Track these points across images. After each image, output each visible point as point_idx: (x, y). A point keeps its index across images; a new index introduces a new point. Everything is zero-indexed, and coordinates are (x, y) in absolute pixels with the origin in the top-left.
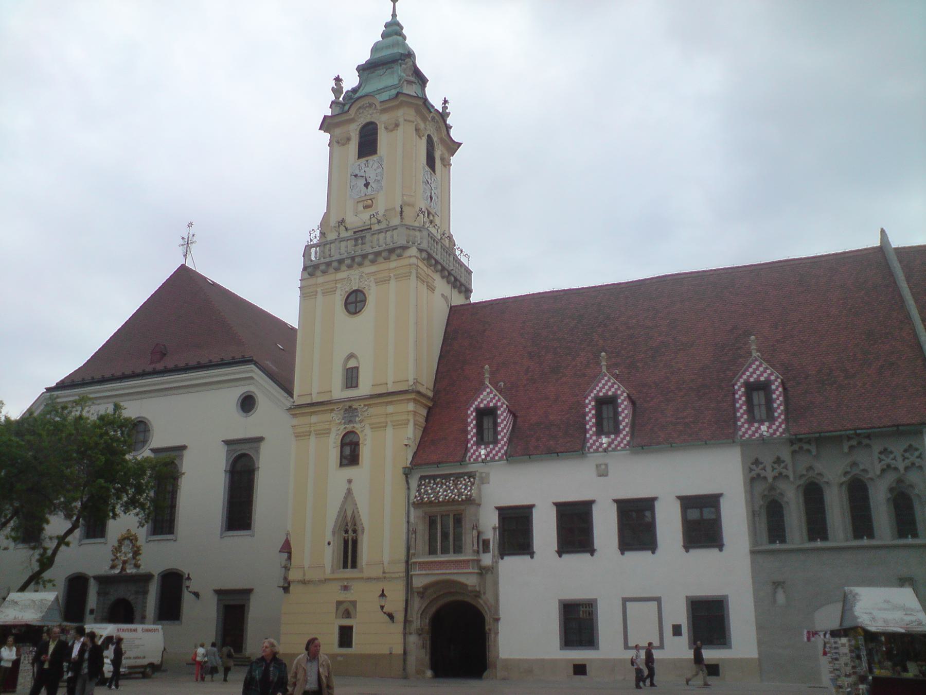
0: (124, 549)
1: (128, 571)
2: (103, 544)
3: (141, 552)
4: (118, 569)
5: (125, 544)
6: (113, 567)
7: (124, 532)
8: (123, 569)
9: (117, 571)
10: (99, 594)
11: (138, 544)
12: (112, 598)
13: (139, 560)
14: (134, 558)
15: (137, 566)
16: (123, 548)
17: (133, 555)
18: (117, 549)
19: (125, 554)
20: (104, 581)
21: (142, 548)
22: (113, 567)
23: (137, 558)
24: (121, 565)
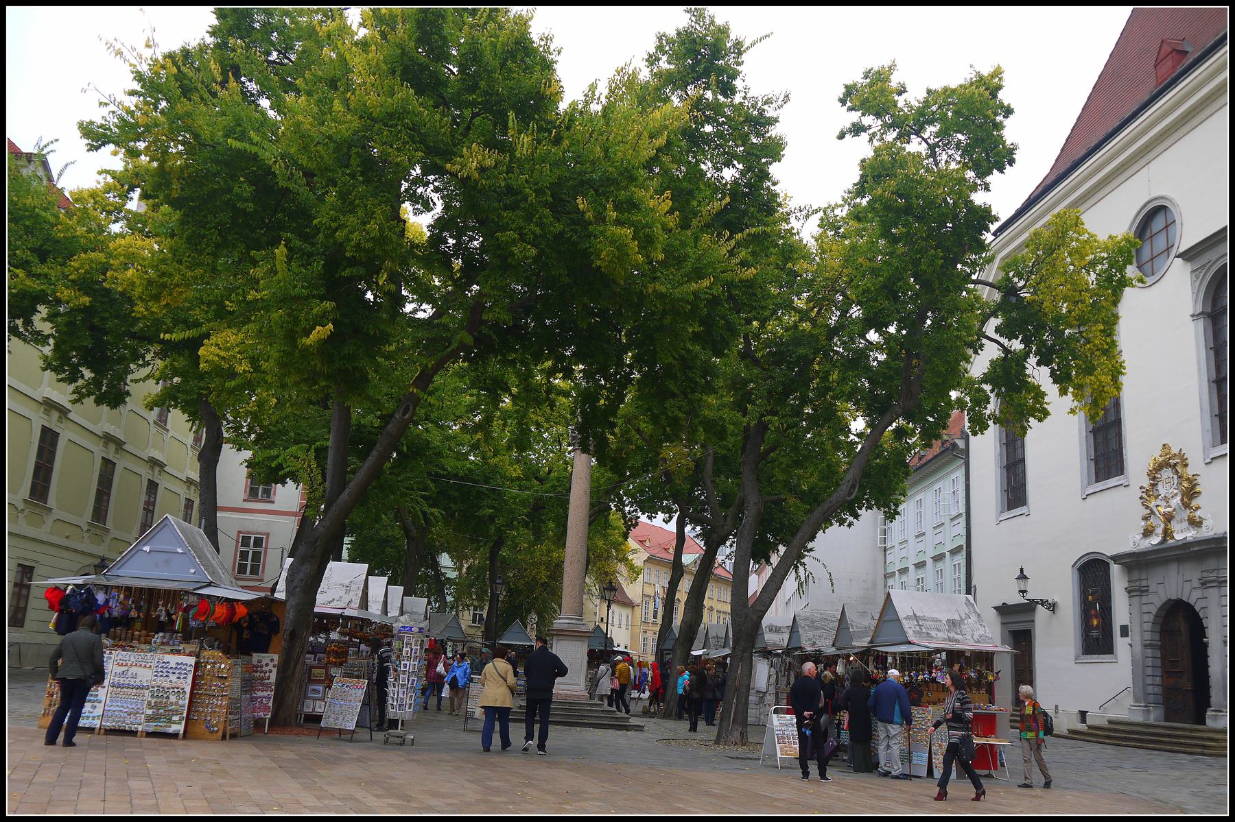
0: (1162, 490)
1: (1178, 537)
2: (1122, 487)
3: (1198, 489)
4: (1157, 535)
5: (1163, 478)
6: (1147, 533)
7: (1157, 453)
8: (1167, 533)
9: (1155, 540)
10: (1129, 591)
11: (1190, 472)
12: (1156, 600)
13: (1198, 508)
14: (1186, 506)
15: (1195, 523)
16: (1160, 487)
17: (1182, 500)
18: (1149, 492)
19: (1166, 499)
20: (1136, 563)
21: (1199, 480)
22: (1147, 533)
23: (1194, 503)
24: (1162, 526)
